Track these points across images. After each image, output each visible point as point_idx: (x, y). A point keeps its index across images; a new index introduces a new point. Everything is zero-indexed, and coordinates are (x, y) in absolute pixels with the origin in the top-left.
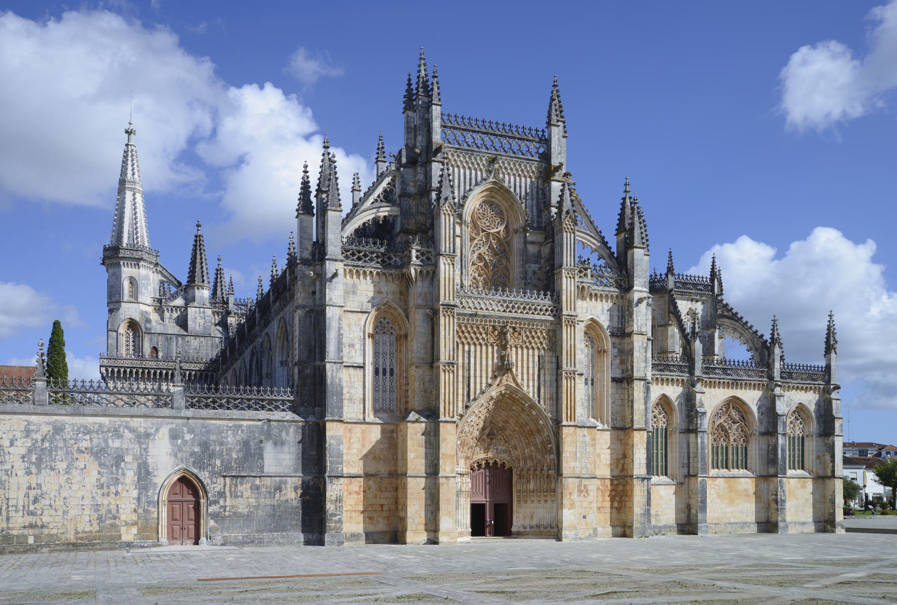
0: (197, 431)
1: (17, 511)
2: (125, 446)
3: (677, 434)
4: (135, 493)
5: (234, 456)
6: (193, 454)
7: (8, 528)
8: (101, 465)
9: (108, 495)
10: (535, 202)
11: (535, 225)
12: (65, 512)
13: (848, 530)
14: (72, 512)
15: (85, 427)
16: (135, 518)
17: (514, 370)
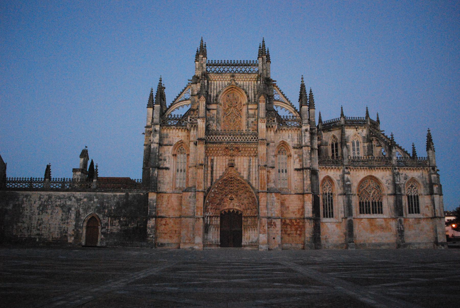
0: (99, 198)
1: (34, 229)
2: (72, 204)
3: (336, 196)
4: (74, 223)
5: (113, 208)
6: (97, 207)
7: (31, 235)
8: (63, 211)
9: (64, 223)
10: (253, 91)
11: (253, 101)
12: (50, 229)
13: (450, 247)
14: (52, 230)
15: (59, 196)
16: (73, 233)
17: (236, 167)
